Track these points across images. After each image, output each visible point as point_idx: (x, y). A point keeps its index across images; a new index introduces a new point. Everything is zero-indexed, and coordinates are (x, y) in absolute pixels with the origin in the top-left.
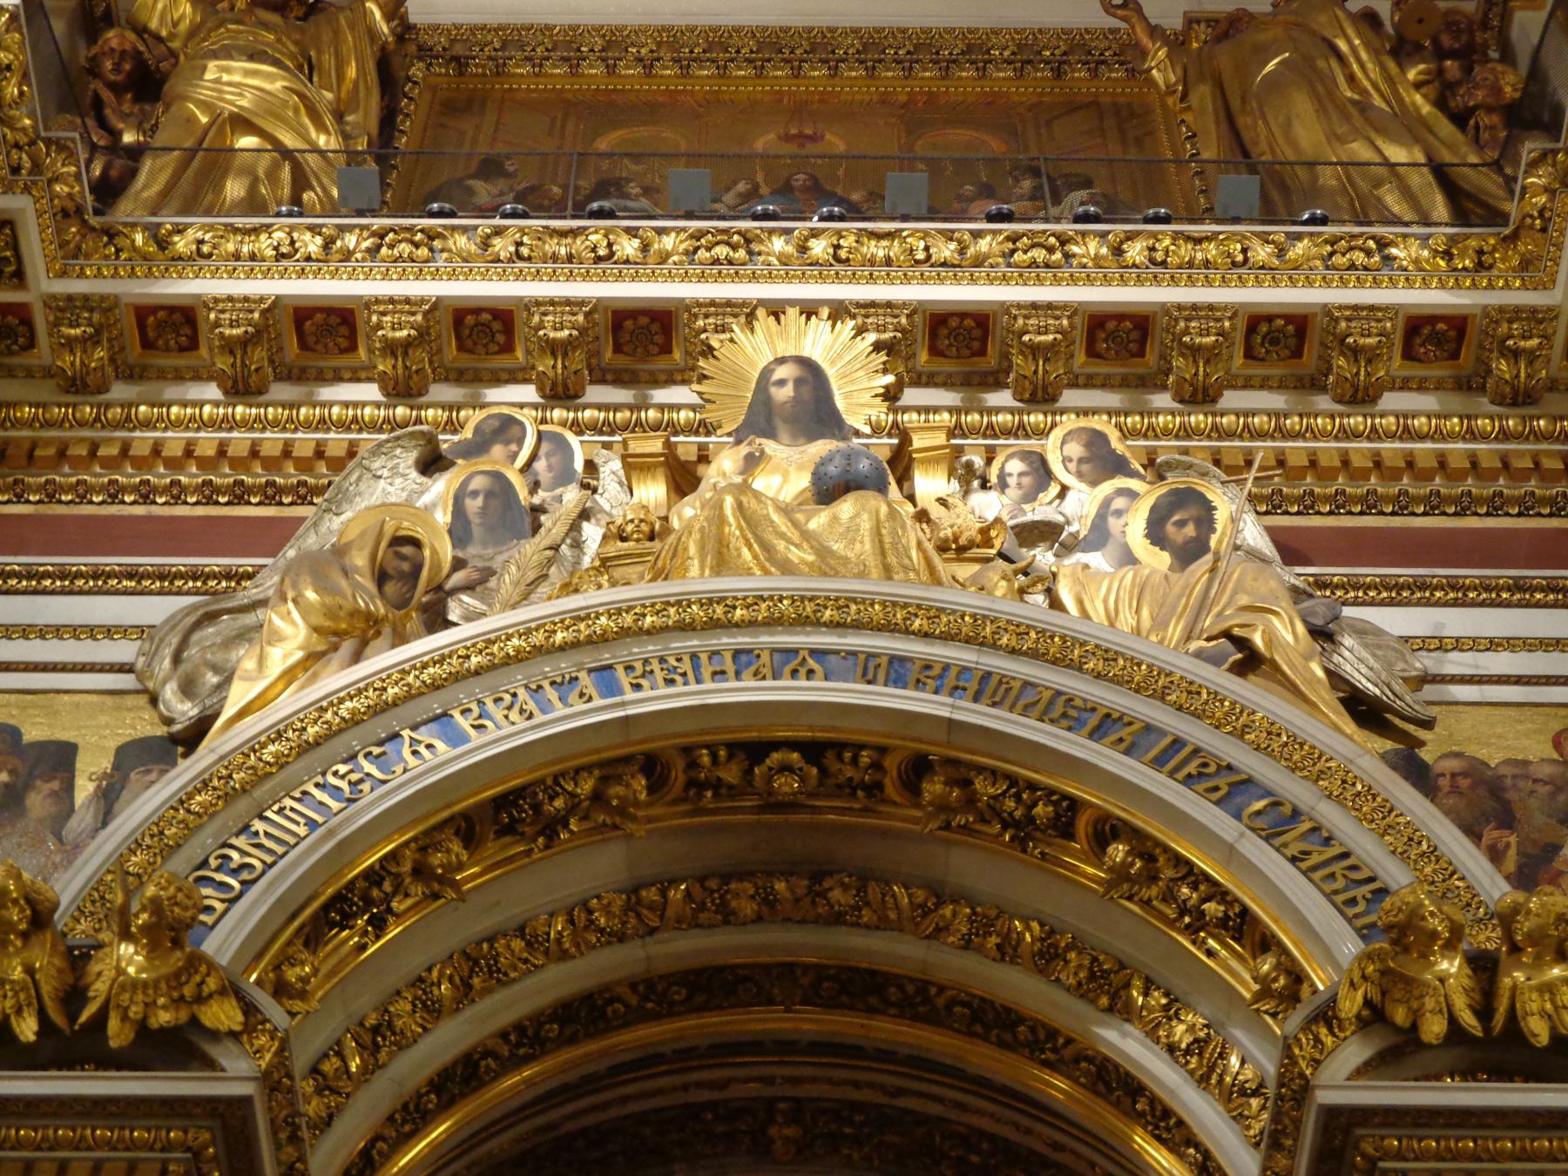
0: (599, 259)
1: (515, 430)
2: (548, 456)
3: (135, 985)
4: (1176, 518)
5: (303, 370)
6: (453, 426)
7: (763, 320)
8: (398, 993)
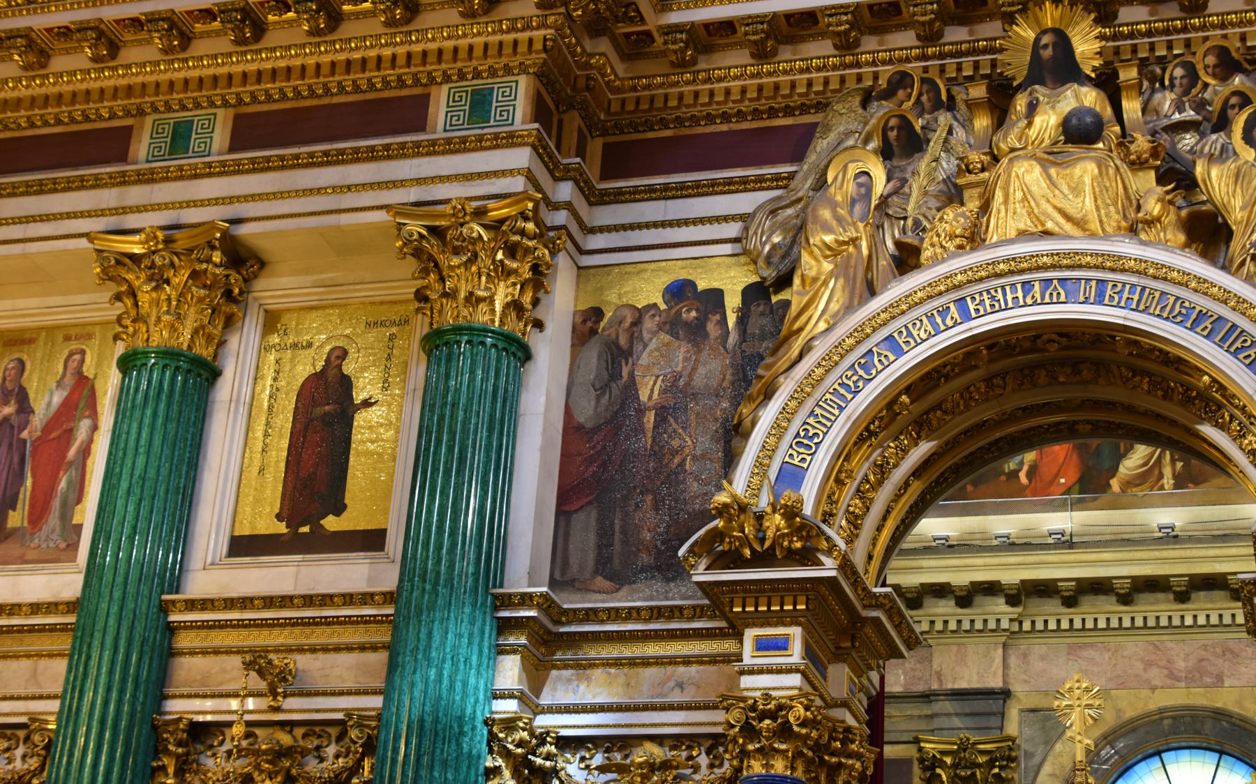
3: (783, 535)
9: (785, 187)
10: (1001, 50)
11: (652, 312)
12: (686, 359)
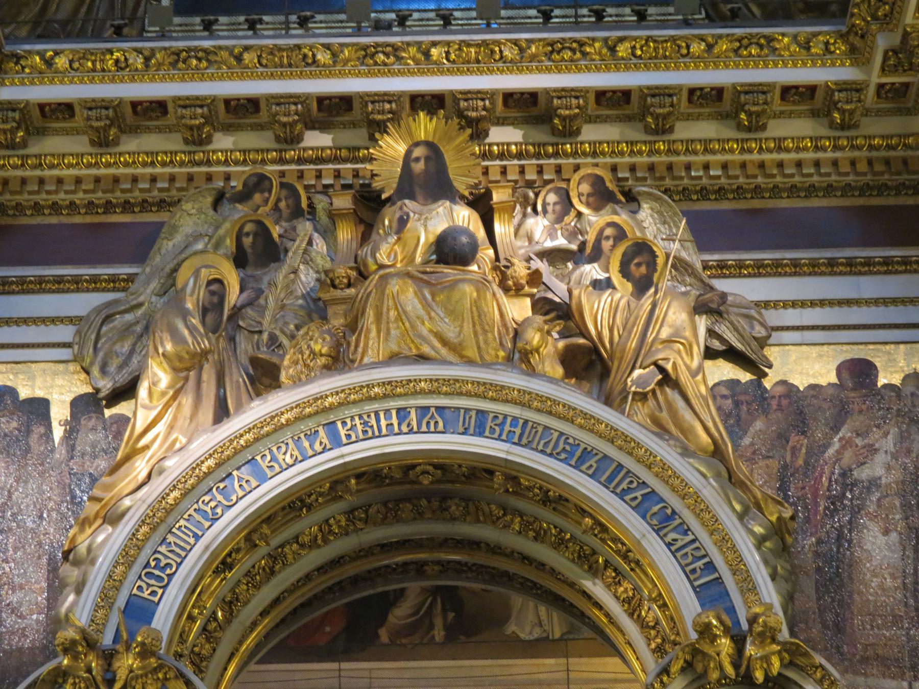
0: (308, 65)
1: (267, 183)
2: (286, 199)
3: (137, 677)
4: (636, 261)
5: (138, 127)
9: (124, 290)
10: (370, 159)
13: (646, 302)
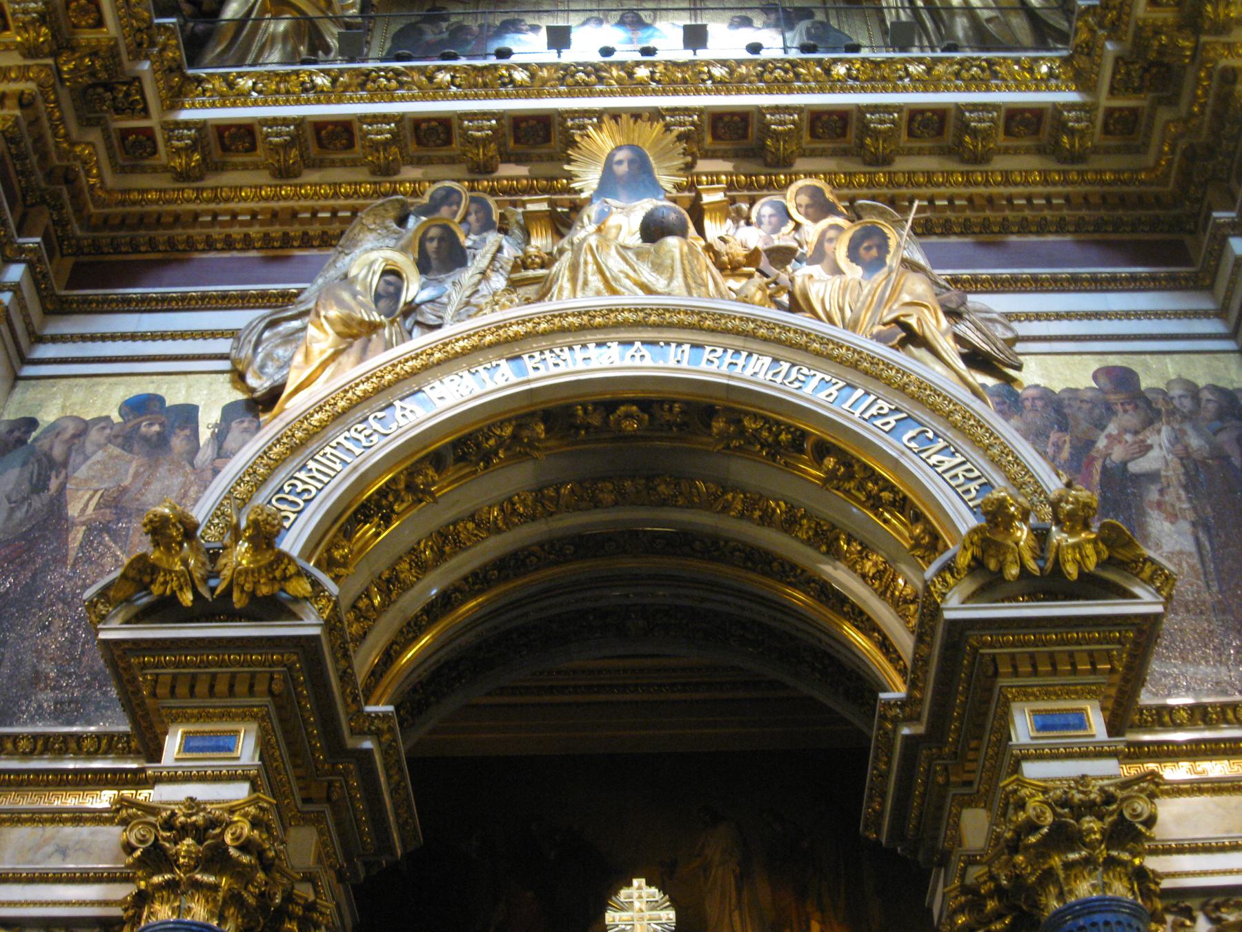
1: (456, 196)
2: (476, 213)
3: (246, 572)
4: (865, 245)
5: (322, 161)
6: (415, 194)
7: (608, 123)
8: (401, 558)
11: (103, 424)
12: (136, 475)
13: (880, 276)
